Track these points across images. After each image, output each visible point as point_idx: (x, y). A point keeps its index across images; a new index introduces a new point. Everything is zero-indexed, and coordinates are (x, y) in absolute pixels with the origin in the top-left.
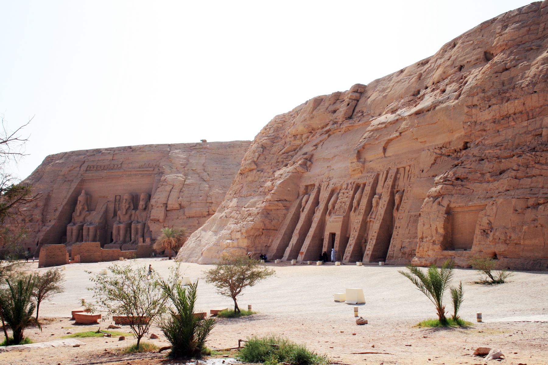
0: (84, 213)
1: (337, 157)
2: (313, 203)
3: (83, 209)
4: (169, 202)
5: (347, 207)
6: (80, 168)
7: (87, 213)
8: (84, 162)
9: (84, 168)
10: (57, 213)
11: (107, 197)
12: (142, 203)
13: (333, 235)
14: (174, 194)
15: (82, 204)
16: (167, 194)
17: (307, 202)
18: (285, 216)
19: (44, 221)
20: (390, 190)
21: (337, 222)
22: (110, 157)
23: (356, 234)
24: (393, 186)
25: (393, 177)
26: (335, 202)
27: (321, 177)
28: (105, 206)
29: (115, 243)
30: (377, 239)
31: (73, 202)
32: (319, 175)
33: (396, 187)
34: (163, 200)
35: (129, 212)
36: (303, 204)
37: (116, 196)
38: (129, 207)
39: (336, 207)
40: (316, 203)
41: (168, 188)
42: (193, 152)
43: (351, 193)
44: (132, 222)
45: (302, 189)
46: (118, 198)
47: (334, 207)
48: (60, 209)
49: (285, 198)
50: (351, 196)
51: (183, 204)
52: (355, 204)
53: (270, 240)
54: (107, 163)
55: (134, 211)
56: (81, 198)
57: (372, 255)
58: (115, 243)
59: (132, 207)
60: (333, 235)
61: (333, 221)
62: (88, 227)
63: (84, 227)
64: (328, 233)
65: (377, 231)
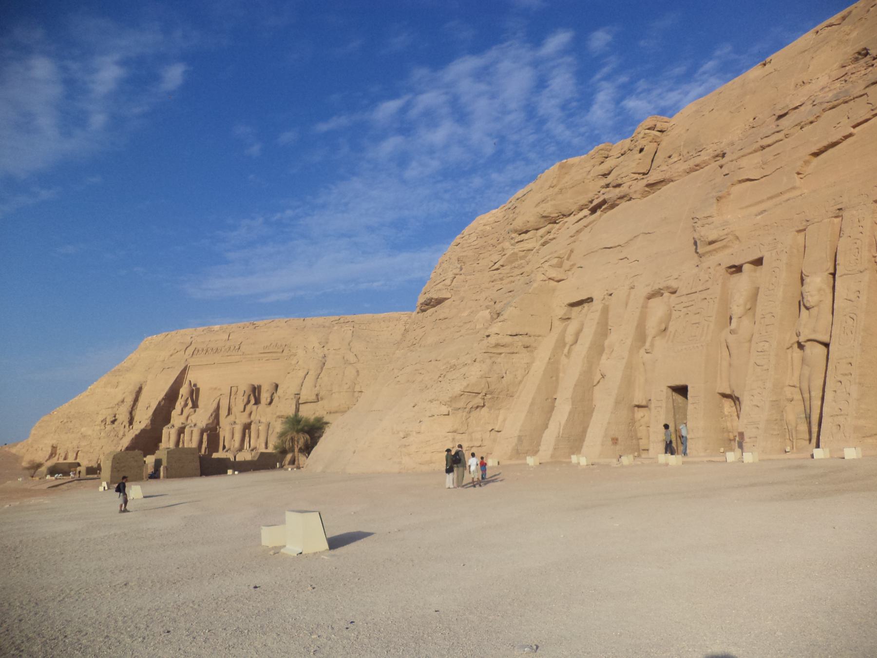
0: (187, 411)
3: (186, 405)
7: (192, 410)
9: (190, 350)
10: (150, 412)
11: (220, 389)
12: (265, 397)
15: (184, 398)
17: (577, 335)
18: (529, 365)
28: (217, 401)
31: (171, 397)
34: (294, 390)
35: (248, 408)
38: (249, 402)
40: (604, 330)
41: (302, 374)
42: (336, 328)
45: (561, 312)
46: (234, 389)
48: (154, 406)
49: (526, 330)
53: (501, 418)
55: (255, 407)
56: (184, 391)
59: (253, 401)
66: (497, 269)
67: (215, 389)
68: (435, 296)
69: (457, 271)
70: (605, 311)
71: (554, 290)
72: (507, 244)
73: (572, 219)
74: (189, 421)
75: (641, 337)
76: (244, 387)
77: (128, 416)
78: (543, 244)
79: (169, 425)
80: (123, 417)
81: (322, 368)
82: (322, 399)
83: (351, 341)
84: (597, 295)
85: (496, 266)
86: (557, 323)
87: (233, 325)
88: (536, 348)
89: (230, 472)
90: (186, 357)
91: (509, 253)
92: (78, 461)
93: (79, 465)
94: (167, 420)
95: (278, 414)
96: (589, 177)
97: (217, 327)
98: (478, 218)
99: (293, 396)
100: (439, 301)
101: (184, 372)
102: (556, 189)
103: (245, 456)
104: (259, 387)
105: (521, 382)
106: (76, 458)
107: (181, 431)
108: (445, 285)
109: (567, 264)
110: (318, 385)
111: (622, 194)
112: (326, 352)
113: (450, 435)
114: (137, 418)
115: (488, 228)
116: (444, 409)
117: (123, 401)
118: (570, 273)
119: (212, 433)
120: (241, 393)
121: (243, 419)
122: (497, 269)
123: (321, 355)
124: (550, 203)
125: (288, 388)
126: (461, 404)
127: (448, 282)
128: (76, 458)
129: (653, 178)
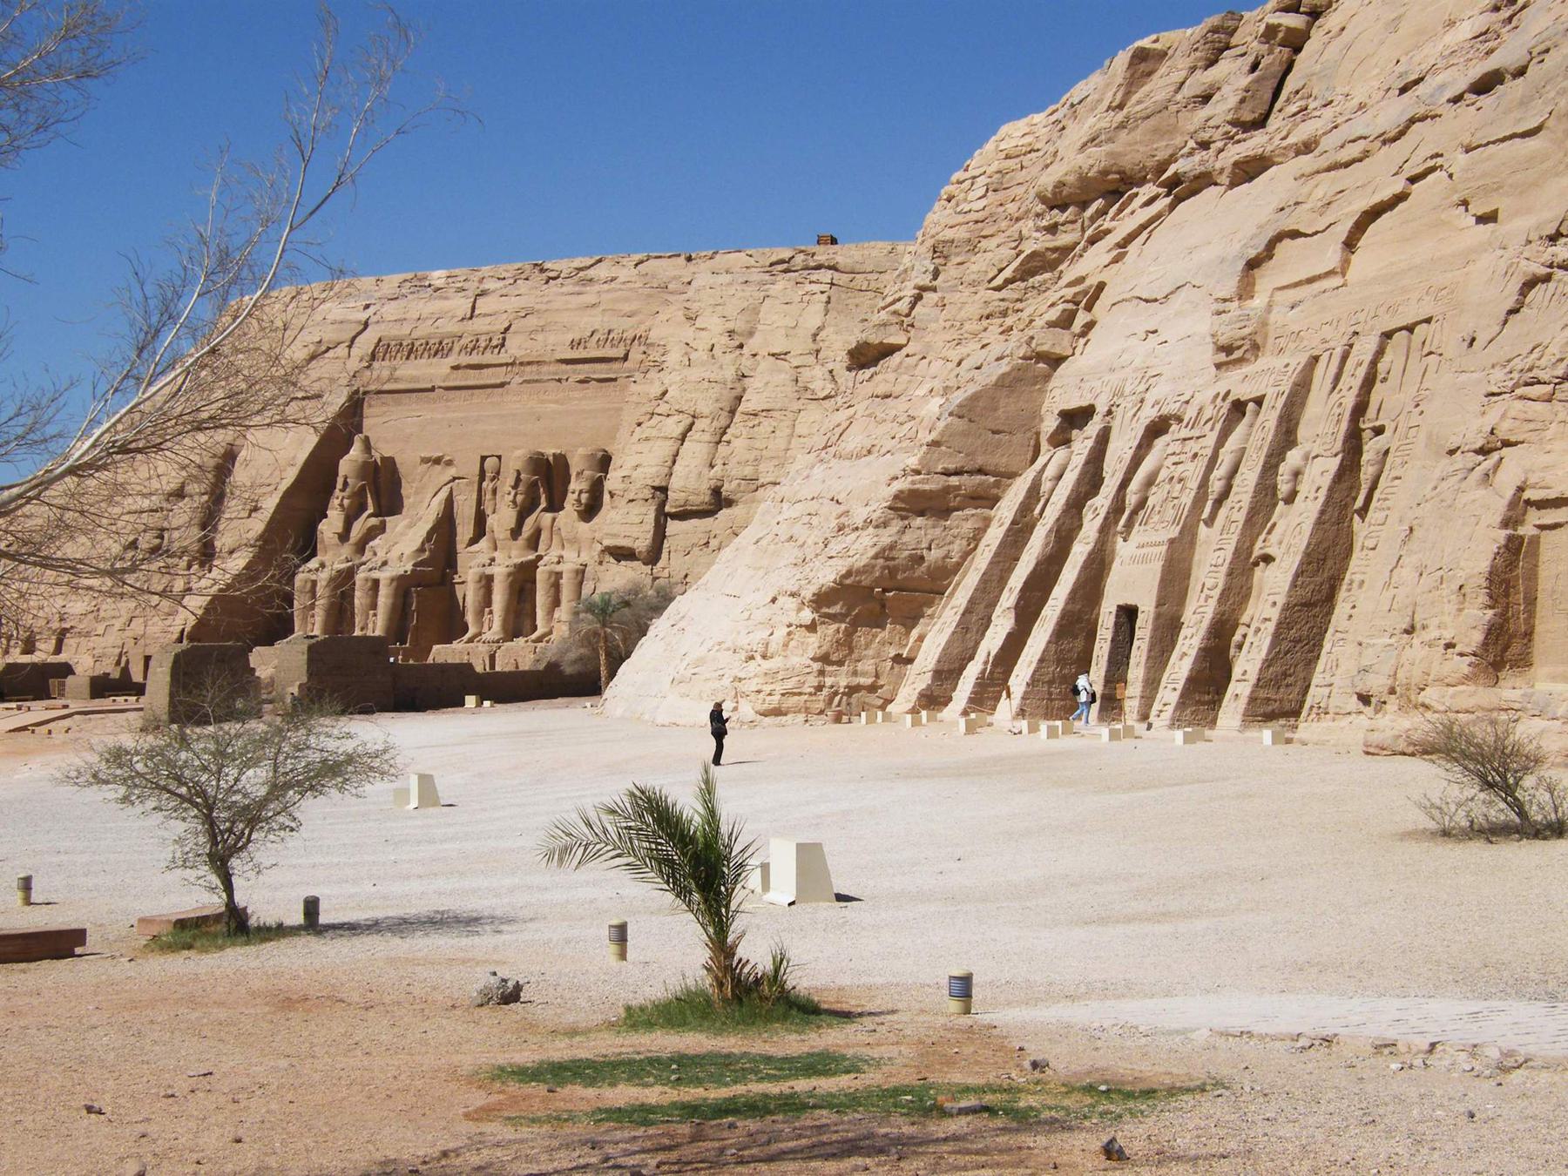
1: (1183, 293)
2: (1079, 482)
4: (675, 483)
5: (1187, 499)
6: (350, 347)
7: (374, 521)
8: (366, 325)
12: (577, 486)
13: (1128, 614)
14: (695, 450)
16: (667, 448)
17: (1059, 477)
18: (976, 537)
19: (206, 554)
20: (1344, 426)
21: (1144, 559)
22: (462, 305)
23: (1209, 611)
24: (1360, 409)
25: (1361, 372)
26: (1150, 482)
27: (1114, 379)
28: (443, 494)
29: (471, 640)
30: (1277, 637)
31: (315, 483)
32: (1112, 370)
33: (1371, 412)
35: (529, 522)
36: (1046, 486)
37: (483, 459)
39: (1150, 503)
40: (1091, 480)
41: (674, 427)
42: (779, 286)
43: (1212, 438)
44: (540, 558)
45: (1050, 424)
46: (490, 464)
47: (1142, 504)
48: (270, 504)
49: (980, 461)
50: (1209, 452)
51: (727, 490)
52: (1216, 486)
54: (449, 327)
55: (549, 516)
56: (349, 464)
57: (1252, 700)
58: (471, 640)
60: (1128, 614)
61: (1133, 559)
62: (375, 574)
63: (360, 577)
64: (1114, 609)
65: (1281, 600)
66: (998, 289)
67: (437, 461)
68: (874, 339)
69: (925, 280)
70: (1103, 438)
71: (1047, 378)
72: (1027, 226)
73: (1148, 190)
74: (368, 554)
75: (1117, 507)
76: (515, 460)
77: (196, 533)
78: (1092, 241)
79: (313, 564)
80: (186, 536)
81: (732, 412)
82: (729, 503)
83: (820, 329)
84: (1101, 408)
85: (999, 281)
86: (1044, 445)
87: (486, 270)
88: (997, 499)
89: (470, 701)
90: (354, 364)
91: (1028, 248)
92: (62, 658)
93: (66, 670)
94: (308, 547)
95: (607, 542)
96: (1179, 97)
97: (438, 276)
98: (1005, 129)
99: (647, 493)
100: (888, 351)
101: (353, 411)
102: (1120, 116)
103: (520, 655)
104: (562, 460)
105: (959, 565)
106: (58, 650)
107: (344, 580)
108: (895, 313)
109: (1082, 318)
110: (719, 462)
111: (1203, 169)
112: (746, 363)
113: (816, 666)
114: (222, 541)
115: (1011, 163)
116: (807, 615)
117: (179, 494)
118: (1082, 341)
119: (431, 594)
120: (508, 480)
121: (517, 554)
122: (998, 289)
123: (729, 374)
124: (1106, 148)
125: (637, 464)
126: (836, 609)
127: (902, 306)
128: (58, 650)
129: (1255, 143)
